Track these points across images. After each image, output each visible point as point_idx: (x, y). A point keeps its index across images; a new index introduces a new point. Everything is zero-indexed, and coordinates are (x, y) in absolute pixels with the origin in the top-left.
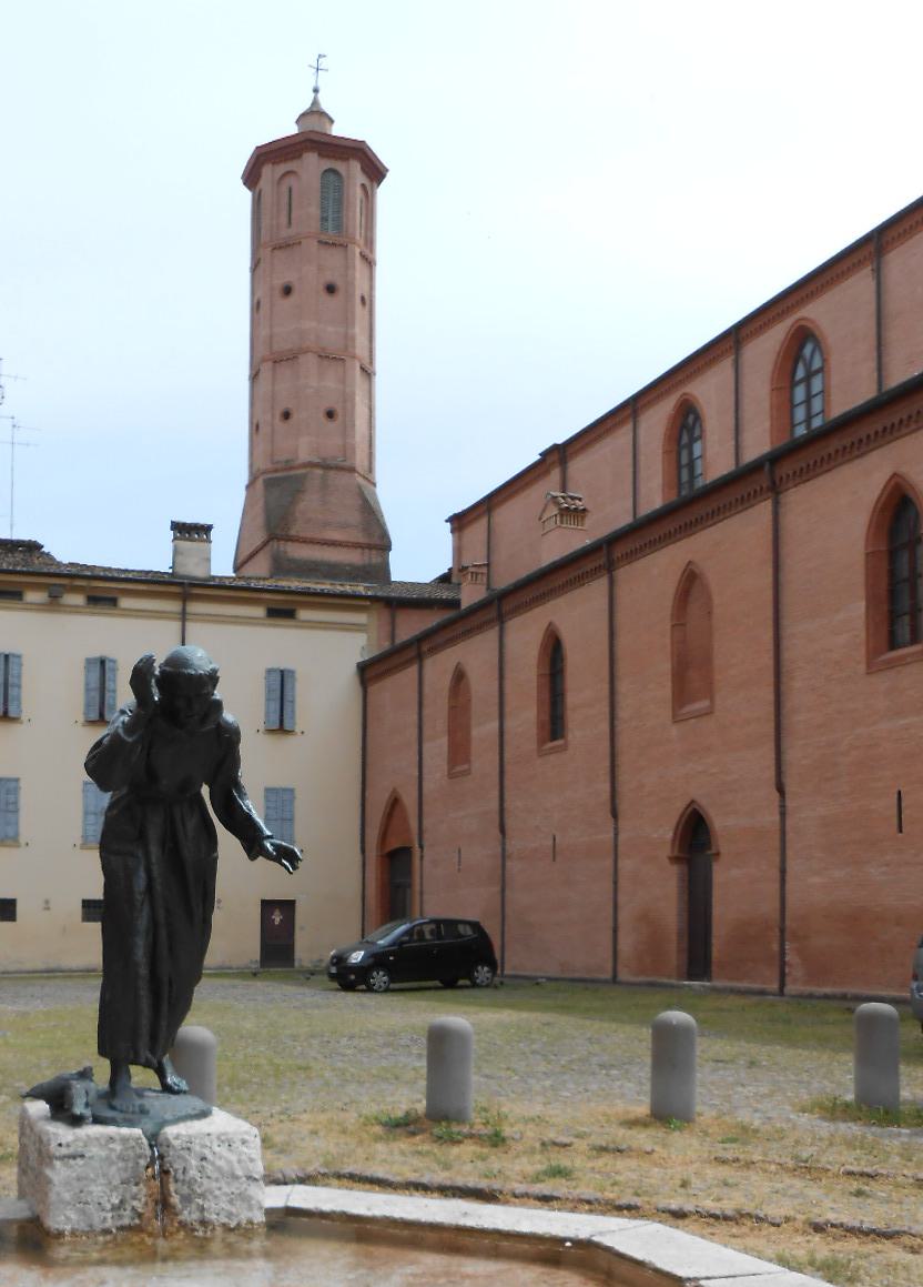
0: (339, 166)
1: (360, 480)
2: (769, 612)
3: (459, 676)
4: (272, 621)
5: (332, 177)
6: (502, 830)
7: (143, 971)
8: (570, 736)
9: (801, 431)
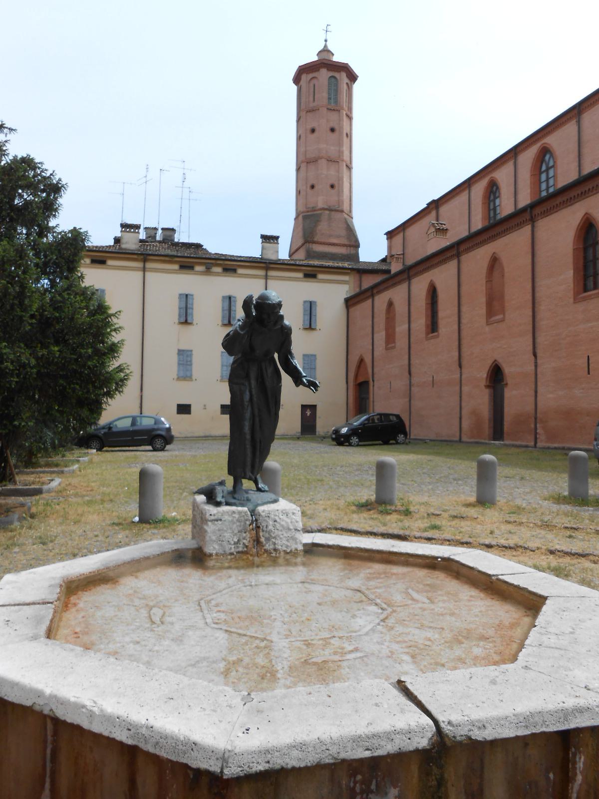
0: (336, 75)
1: (346, 216)
2: (530, 275)
3: (390, 304)
4: (306, 279)
5: (333, 80)
6: (410, 373)
7: (248, 437)
8: (440, 331)
9: (544, 194)
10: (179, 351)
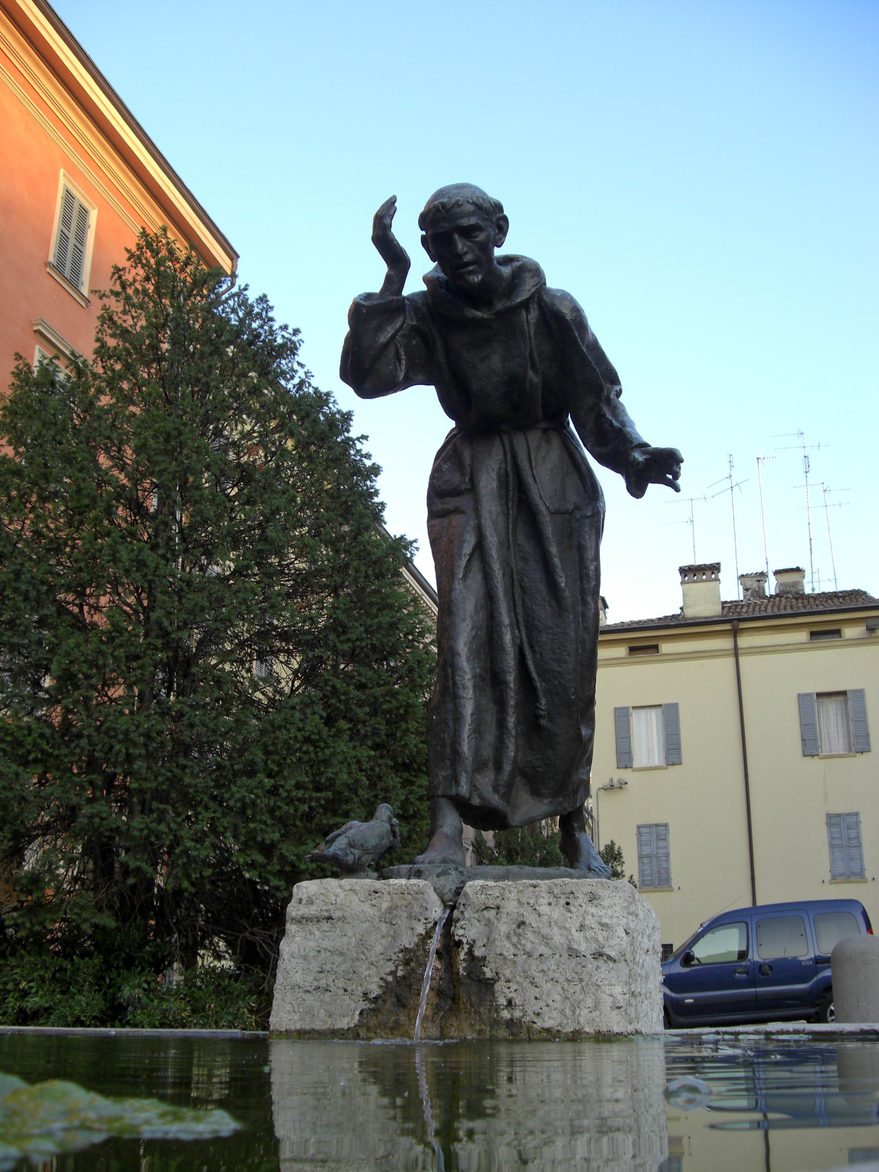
10: (829, 816)
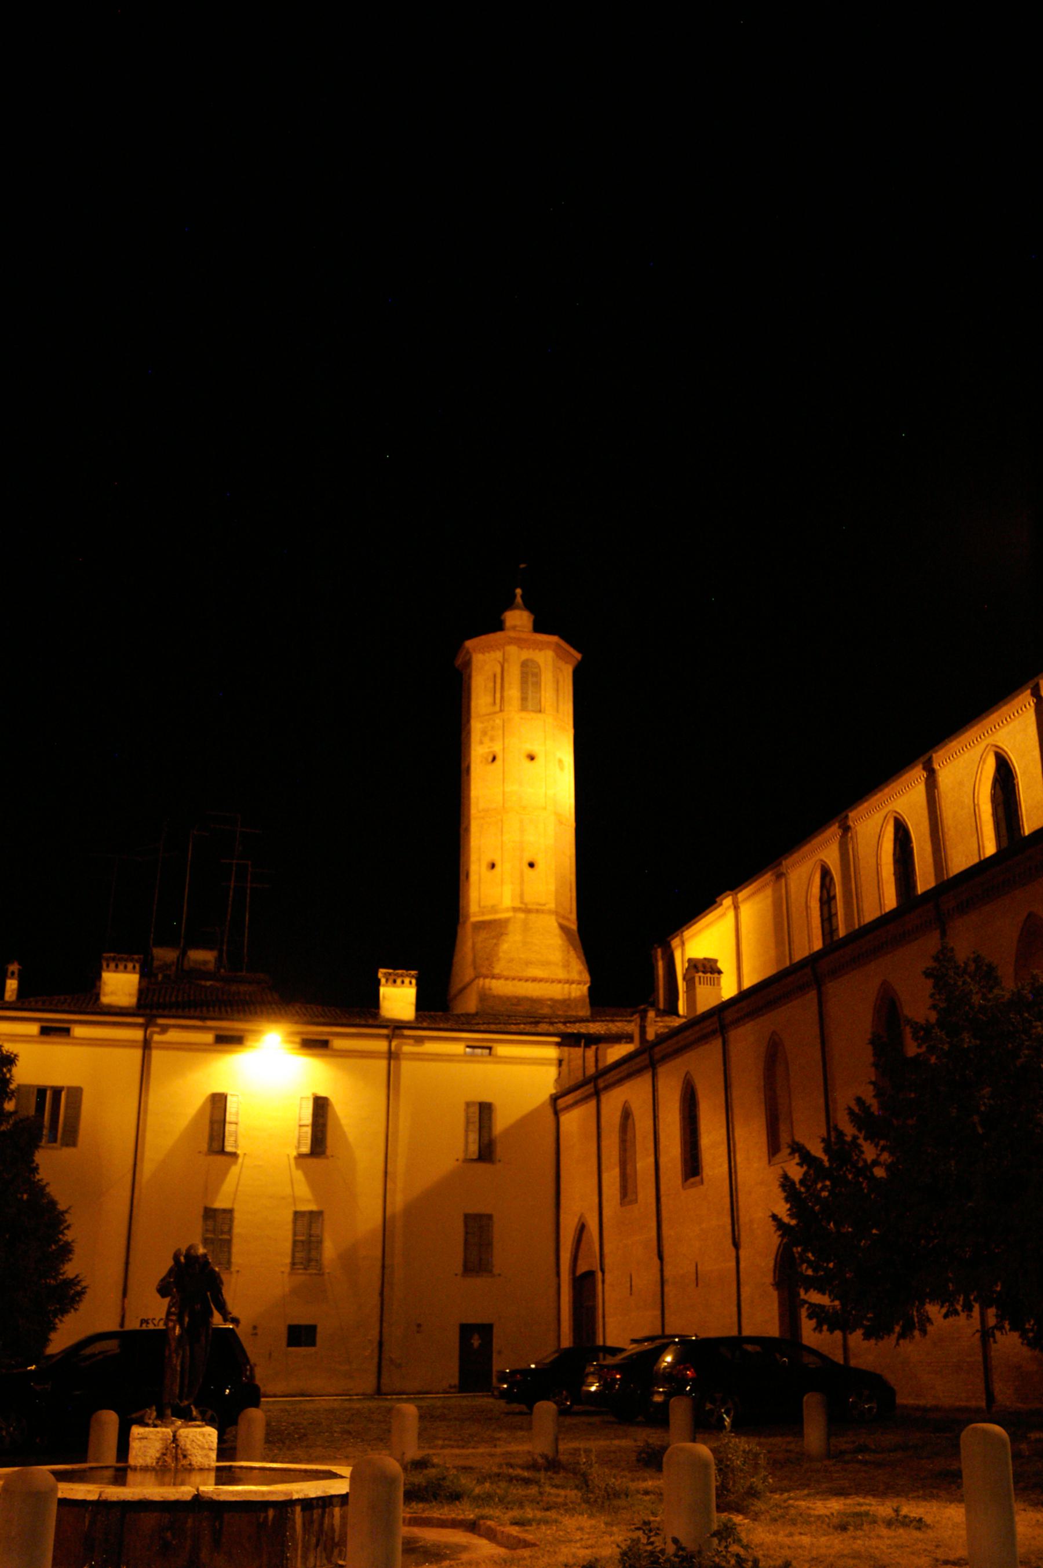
3: (627, 1115)
8: (704, 1175)
